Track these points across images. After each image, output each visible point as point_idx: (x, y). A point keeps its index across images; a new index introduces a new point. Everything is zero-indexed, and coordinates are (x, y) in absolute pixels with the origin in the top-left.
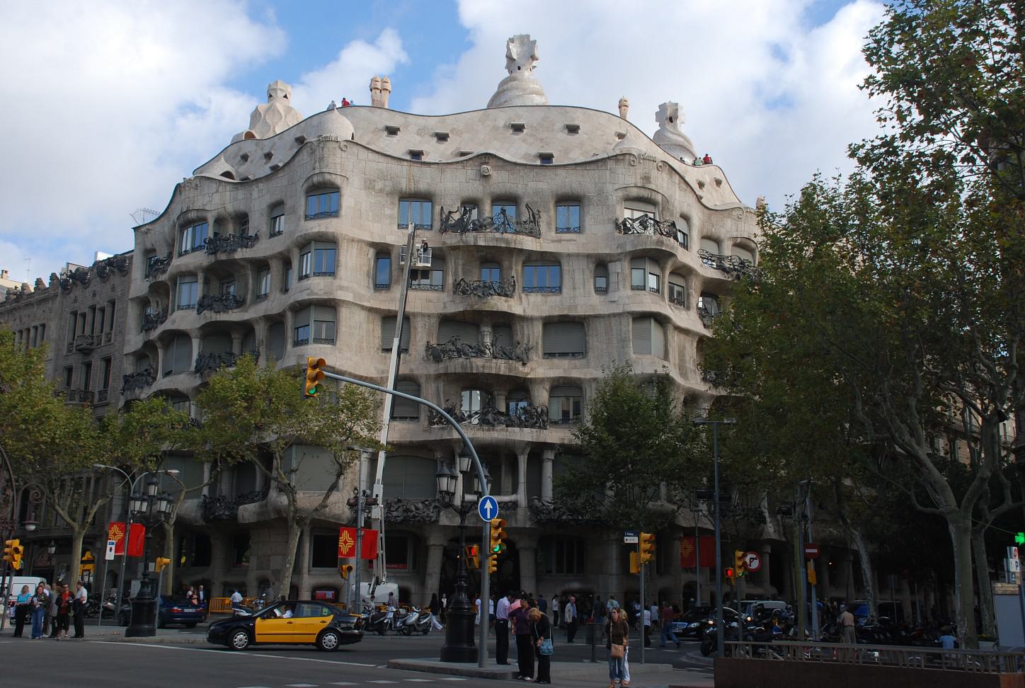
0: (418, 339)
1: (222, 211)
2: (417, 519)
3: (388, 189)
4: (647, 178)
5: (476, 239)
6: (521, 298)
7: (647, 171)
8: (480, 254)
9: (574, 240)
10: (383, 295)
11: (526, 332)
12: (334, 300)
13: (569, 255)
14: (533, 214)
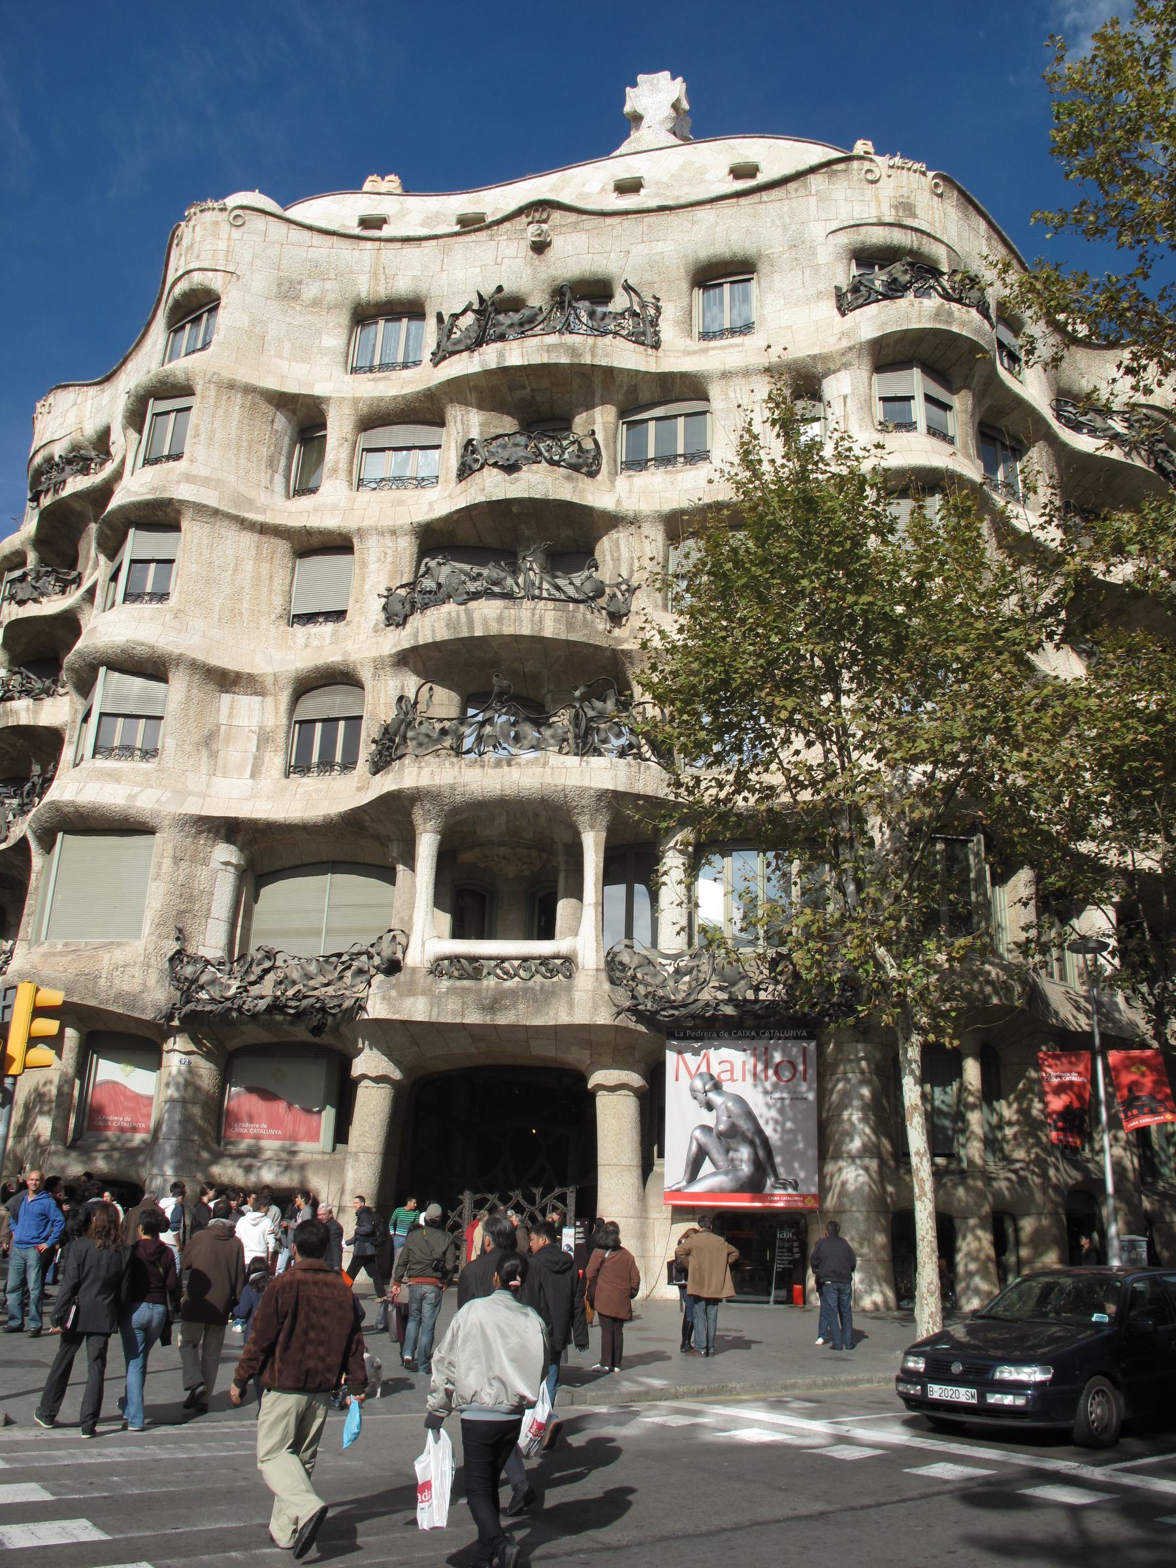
0: (367, 587)
1: (76, 436)
2: (305, 1002)
3: (330, 298)
4: (907, 207)
5: (501, 355)
6: (613, 482)
7: (905, 192)
8: (518, 394)
9: (737, 345)
10: (305, 502)
11: (625, 553)
12: (170, 501)
13: (725, 375)
14: (644, 306)
